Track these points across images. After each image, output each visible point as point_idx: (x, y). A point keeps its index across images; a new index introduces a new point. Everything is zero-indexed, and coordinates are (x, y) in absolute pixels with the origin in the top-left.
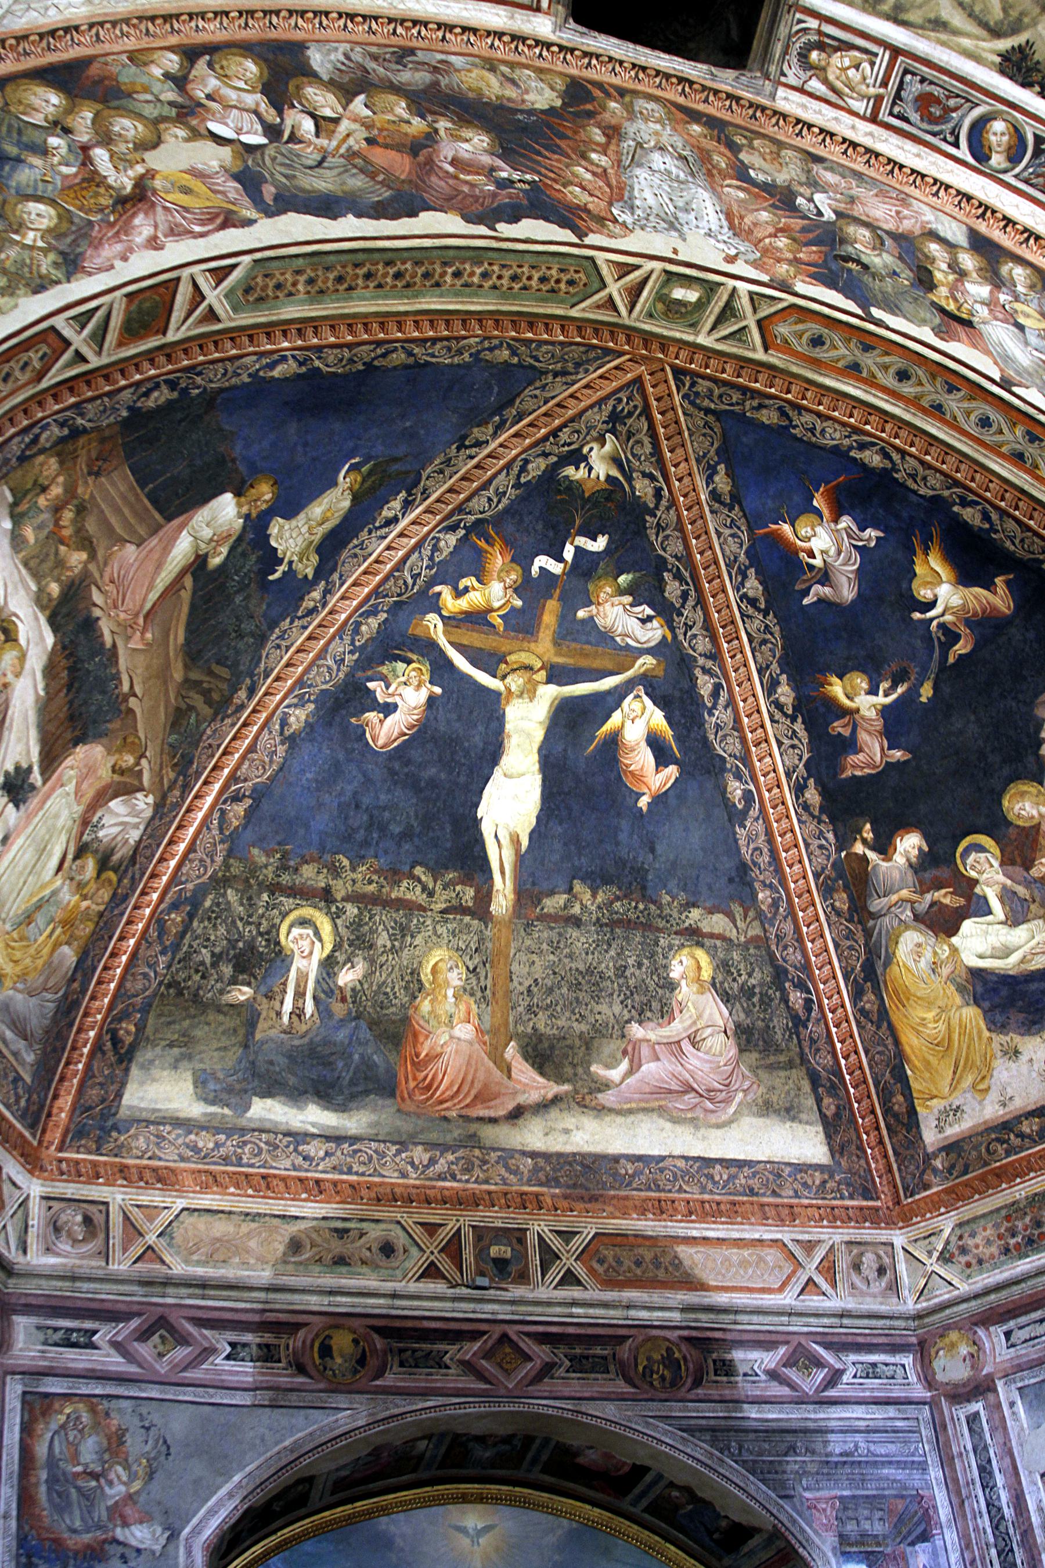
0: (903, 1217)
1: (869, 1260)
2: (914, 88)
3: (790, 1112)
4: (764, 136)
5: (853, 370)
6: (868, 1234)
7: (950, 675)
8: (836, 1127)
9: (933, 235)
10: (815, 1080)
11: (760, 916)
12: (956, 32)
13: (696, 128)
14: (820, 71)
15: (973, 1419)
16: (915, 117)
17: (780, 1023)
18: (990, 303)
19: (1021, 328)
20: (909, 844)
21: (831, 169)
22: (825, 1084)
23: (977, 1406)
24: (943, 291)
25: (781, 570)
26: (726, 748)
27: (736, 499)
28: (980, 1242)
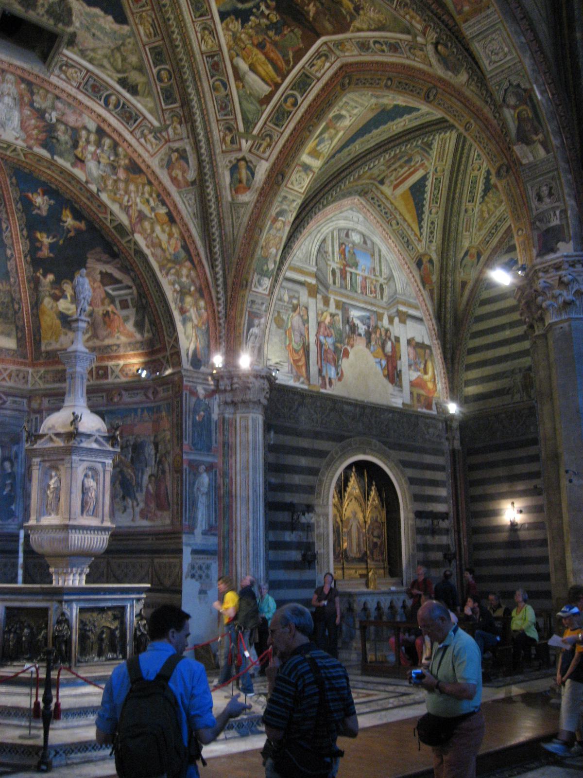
0: (33, 365)
1: (21, 375)
2: (91, 82)
3: (8, 335)
4: (44, 89)
5: (49, 168)
6: (23, 368)
7: (67, 240)
8: (20, 341)
9: (85, 128)
10: (17, 328)
11: (11, 285)
12: (107, 69)
13: (23, 86)
14: (65, 73)
15: (36, 419)
16: (90, 90)
17: (11, 312)
18: (94, 154)
19: (99, 162)
20: (51, 277)
21: (62, 102)
22: (20, 329)
23: (38, 416)
24: (80, 149)
25: (27, 205)
26: (8, 242)
27: (17, 185)
28: (49, 377)
